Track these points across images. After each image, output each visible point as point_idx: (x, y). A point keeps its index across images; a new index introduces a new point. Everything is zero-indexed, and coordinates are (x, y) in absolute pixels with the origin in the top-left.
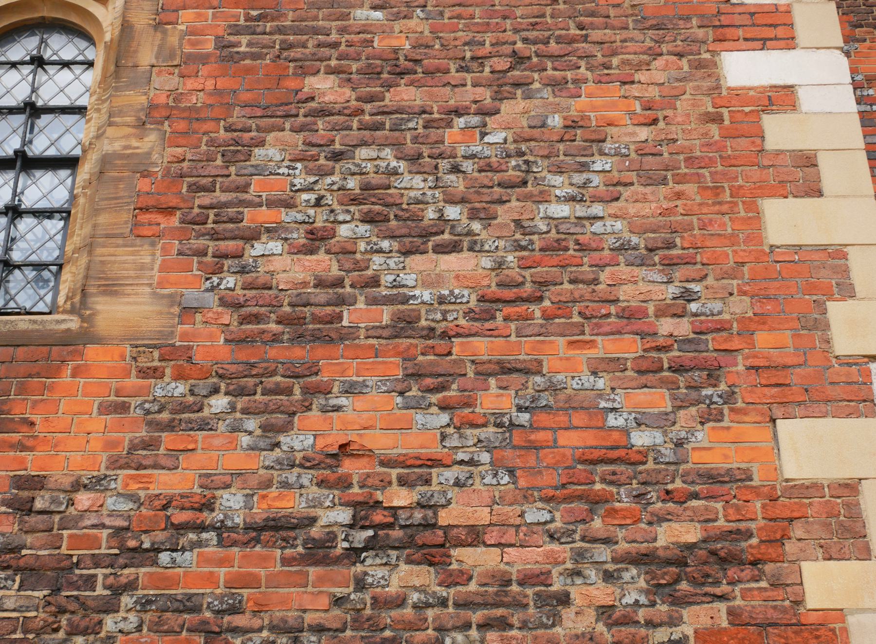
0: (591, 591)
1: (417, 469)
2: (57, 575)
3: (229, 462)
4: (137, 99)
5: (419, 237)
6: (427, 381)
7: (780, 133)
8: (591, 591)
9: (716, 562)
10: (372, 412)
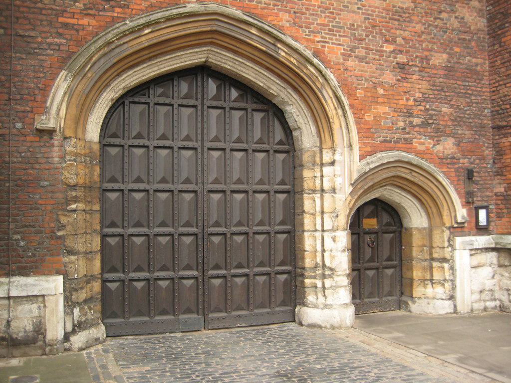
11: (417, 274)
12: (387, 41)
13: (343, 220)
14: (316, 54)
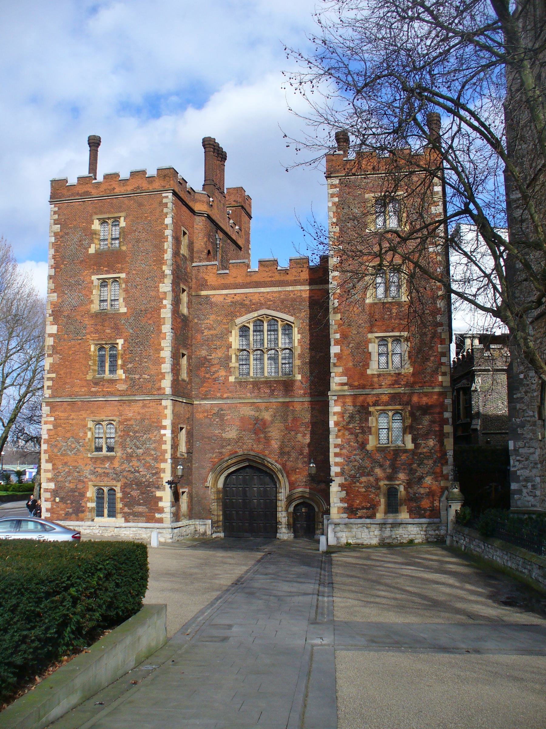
0: (148, 476)
3: (126, 466)
5: (138, 448)
6: (139, 460)
8: (148, 476)
9: (157, 473)
13: (284, 509)
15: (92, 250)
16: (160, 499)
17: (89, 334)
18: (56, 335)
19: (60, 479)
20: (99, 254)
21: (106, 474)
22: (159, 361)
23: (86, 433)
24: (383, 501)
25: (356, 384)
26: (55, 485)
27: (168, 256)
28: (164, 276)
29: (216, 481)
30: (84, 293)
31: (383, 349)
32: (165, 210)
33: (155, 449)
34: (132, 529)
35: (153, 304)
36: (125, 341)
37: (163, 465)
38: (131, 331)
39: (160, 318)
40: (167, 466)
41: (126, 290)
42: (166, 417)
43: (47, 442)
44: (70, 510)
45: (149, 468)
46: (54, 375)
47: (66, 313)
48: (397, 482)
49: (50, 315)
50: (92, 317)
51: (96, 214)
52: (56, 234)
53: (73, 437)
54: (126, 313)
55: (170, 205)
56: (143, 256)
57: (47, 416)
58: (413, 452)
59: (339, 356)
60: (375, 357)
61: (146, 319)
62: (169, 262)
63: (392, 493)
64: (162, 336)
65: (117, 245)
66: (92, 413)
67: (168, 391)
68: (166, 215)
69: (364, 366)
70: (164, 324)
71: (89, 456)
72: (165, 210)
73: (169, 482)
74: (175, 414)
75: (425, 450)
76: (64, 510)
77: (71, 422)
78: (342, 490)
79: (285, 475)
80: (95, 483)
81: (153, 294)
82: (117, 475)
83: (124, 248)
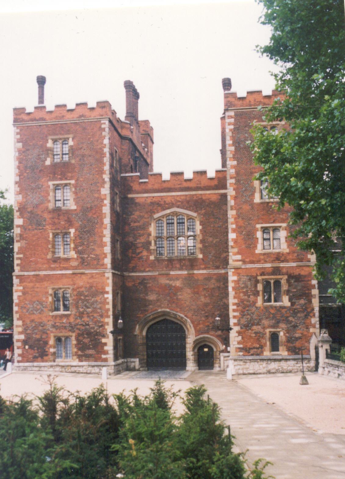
1: (88, 321)
2: (72, 327)
3: (79, 321)
4: (72, 298)
5: (88, 308)
6: (88, 317)
7: (107, 301)
9: (102, 326)
10: (86, 319)
11: (215, 361)
12: (203, 311)
13: (191, 349)
14: (186, 316)
15: (48, 162)
16: (105, 344)
17: (48, 225)
18: (22, 226)
19: (28, 331)
20: (54, 166)
21: (65, 328)
22: (103, 245)
23: (47, 298)
24: (268, 343)
25: (247, 260)
26: (25, 336)
27: (107, 168)
28: (104, 182)
29: (141, 331)
30: (43, 194)
31: (266, 236)
32: (104, 133)
33: (100, 308)
34: (84, 367)
35: (96, 203)
36: (76, 230)
37: (106, 320)
38: (80, 223)
39: (102, 214)
40: (110, 320)
41: (75, 193)
42: (108, 285)
43: (17, 305)
44: (37, 355)
45: (96, 322)
46: (21, 256)
47: (29, 210)
48: (278, 330)
49: (17, 211)
50: (50, 212)
51: (50, 135)
52: (19, 151)
53: (38, 301)
54: (76, 210)
55: (107, 130)
56: (88, 167)
57: (18, 285)
58: (289, 309)
59: (235, 241)
60: (260, 241)
61: (91, 214)
62: (108, 172)
63: (274, 337)
64: (104, 226)
65: (67, 159)
66: (52, 283)
67: (109, 266)
68: (104, 137)
69: (253, 247)
70: (105, 217)
71: (51, 314)
72: (104, 133)
73: (111, 332)
74: (115, 284)
75: (298, 307)
76: (32, 354)
77: (36, 289)
78: (239, 335)
79: (192, 325)
80: (56, 334)
81: (96, 195)
82: (72, 328)
83: (73, 161)
